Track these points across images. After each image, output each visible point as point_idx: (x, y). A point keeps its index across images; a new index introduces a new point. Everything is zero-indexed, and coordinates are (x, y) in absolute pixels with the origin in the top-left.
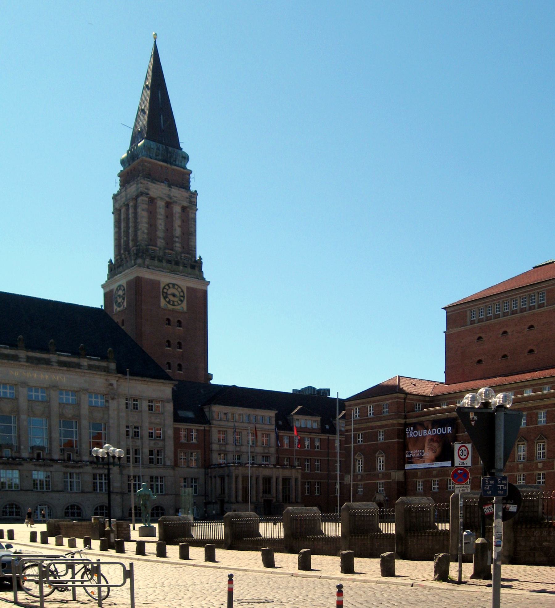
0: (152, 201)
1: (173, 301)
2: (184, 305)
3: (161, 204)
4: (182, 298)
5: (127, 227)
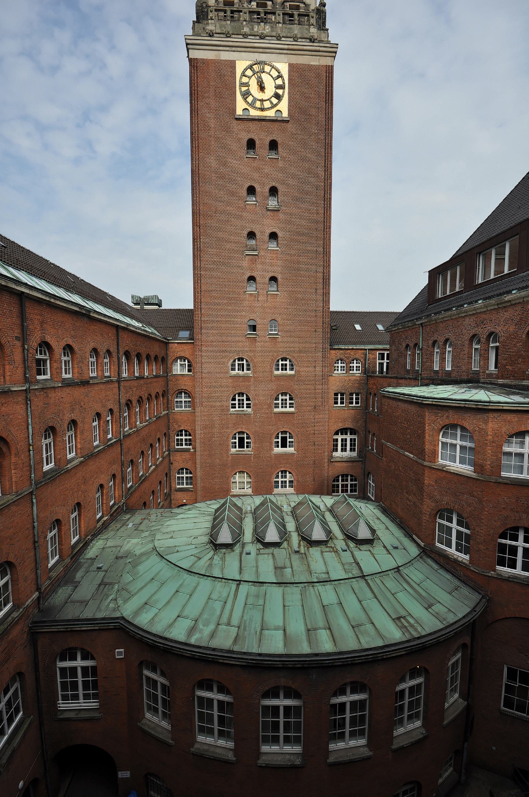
1: (262, 101)
2: (284, 106)
4: (280, 92)
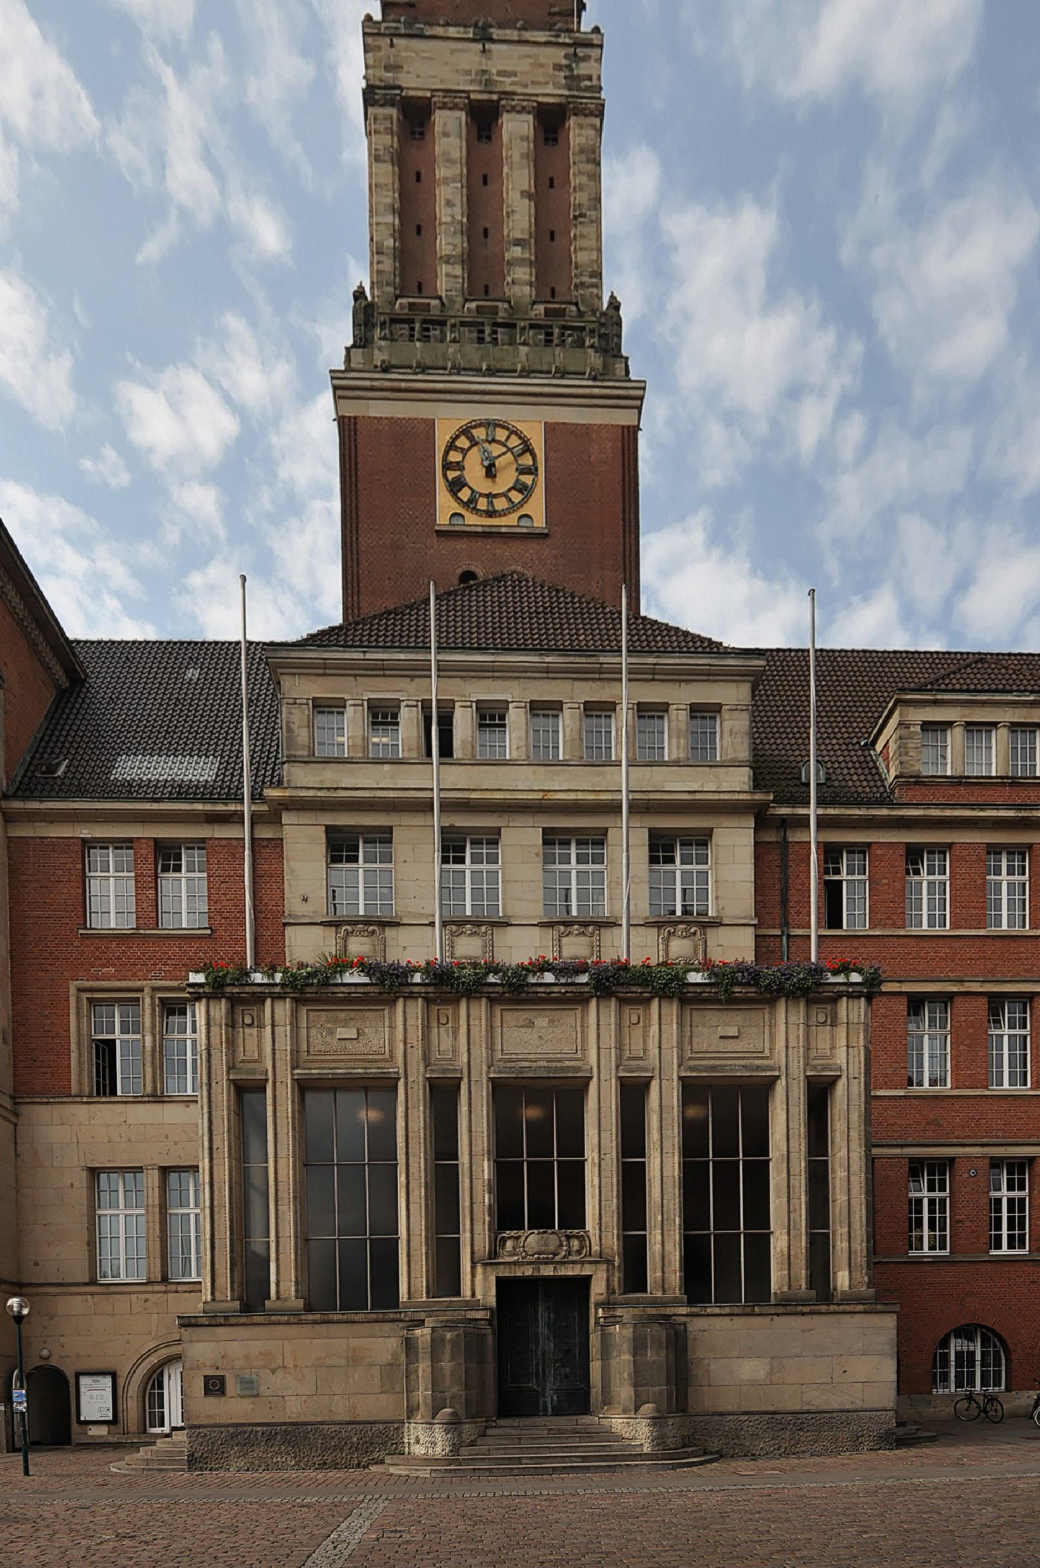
1: (490, 496)
2: (537, 510)
3: (449, 131)
4: (527, 479)
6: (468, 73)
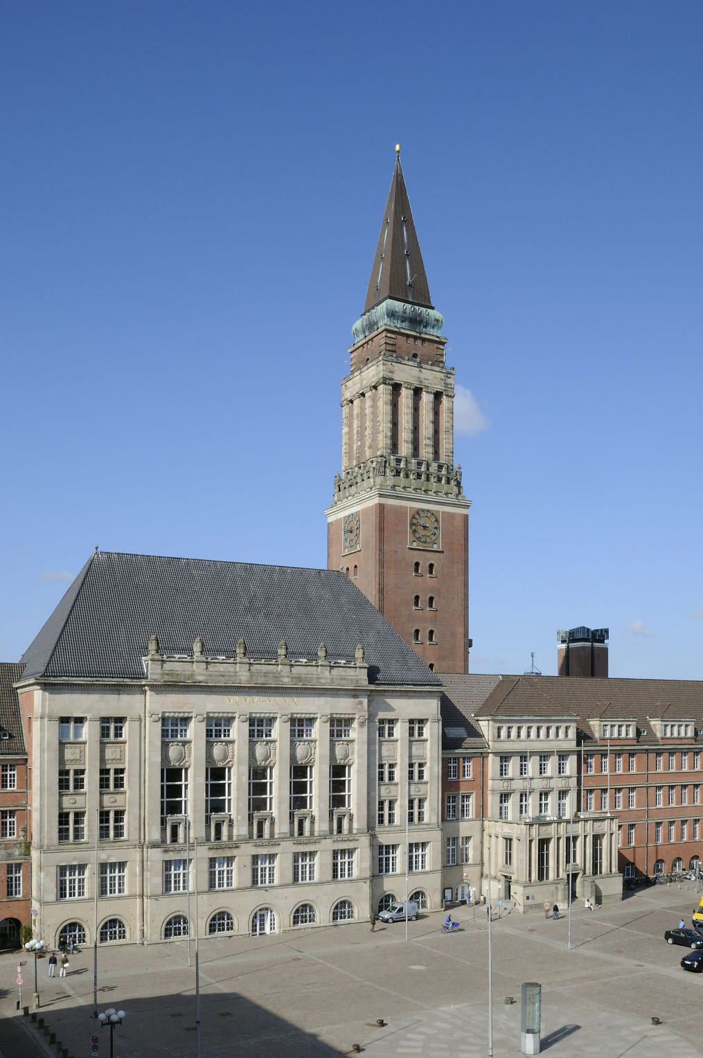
0: (396, 388)
5: (362, 427)
6: (414, 377)
